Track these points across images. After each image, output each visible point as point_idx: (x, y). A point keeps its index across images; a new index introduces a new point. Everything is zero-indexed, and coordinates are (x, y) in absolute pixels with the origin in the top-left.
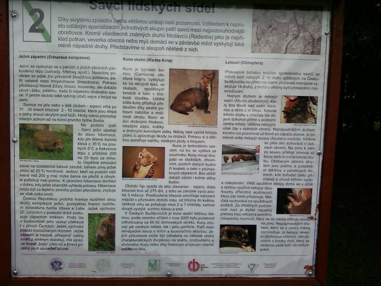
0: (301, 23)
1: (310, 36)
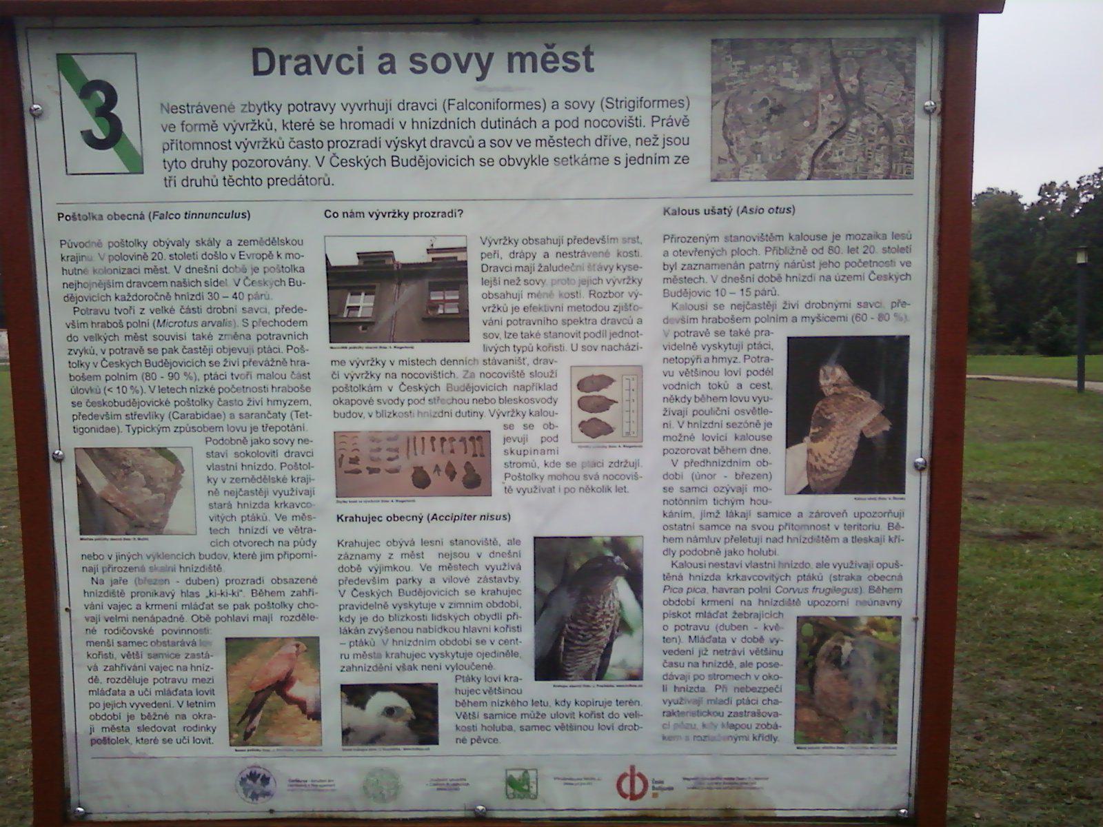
0: (854, 91)
1: (879, 127)
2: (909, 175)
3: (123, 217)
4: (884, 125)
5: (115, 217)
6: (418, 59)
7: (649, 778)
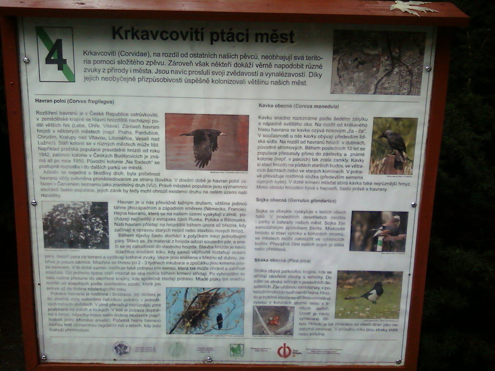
0: (397, 55)
1: (407, 72)
2: (418, 93)
3: (282, 106)
4: (409, 71)
5: (55, 101)
6: (284, 36)
7: (292, 349)
